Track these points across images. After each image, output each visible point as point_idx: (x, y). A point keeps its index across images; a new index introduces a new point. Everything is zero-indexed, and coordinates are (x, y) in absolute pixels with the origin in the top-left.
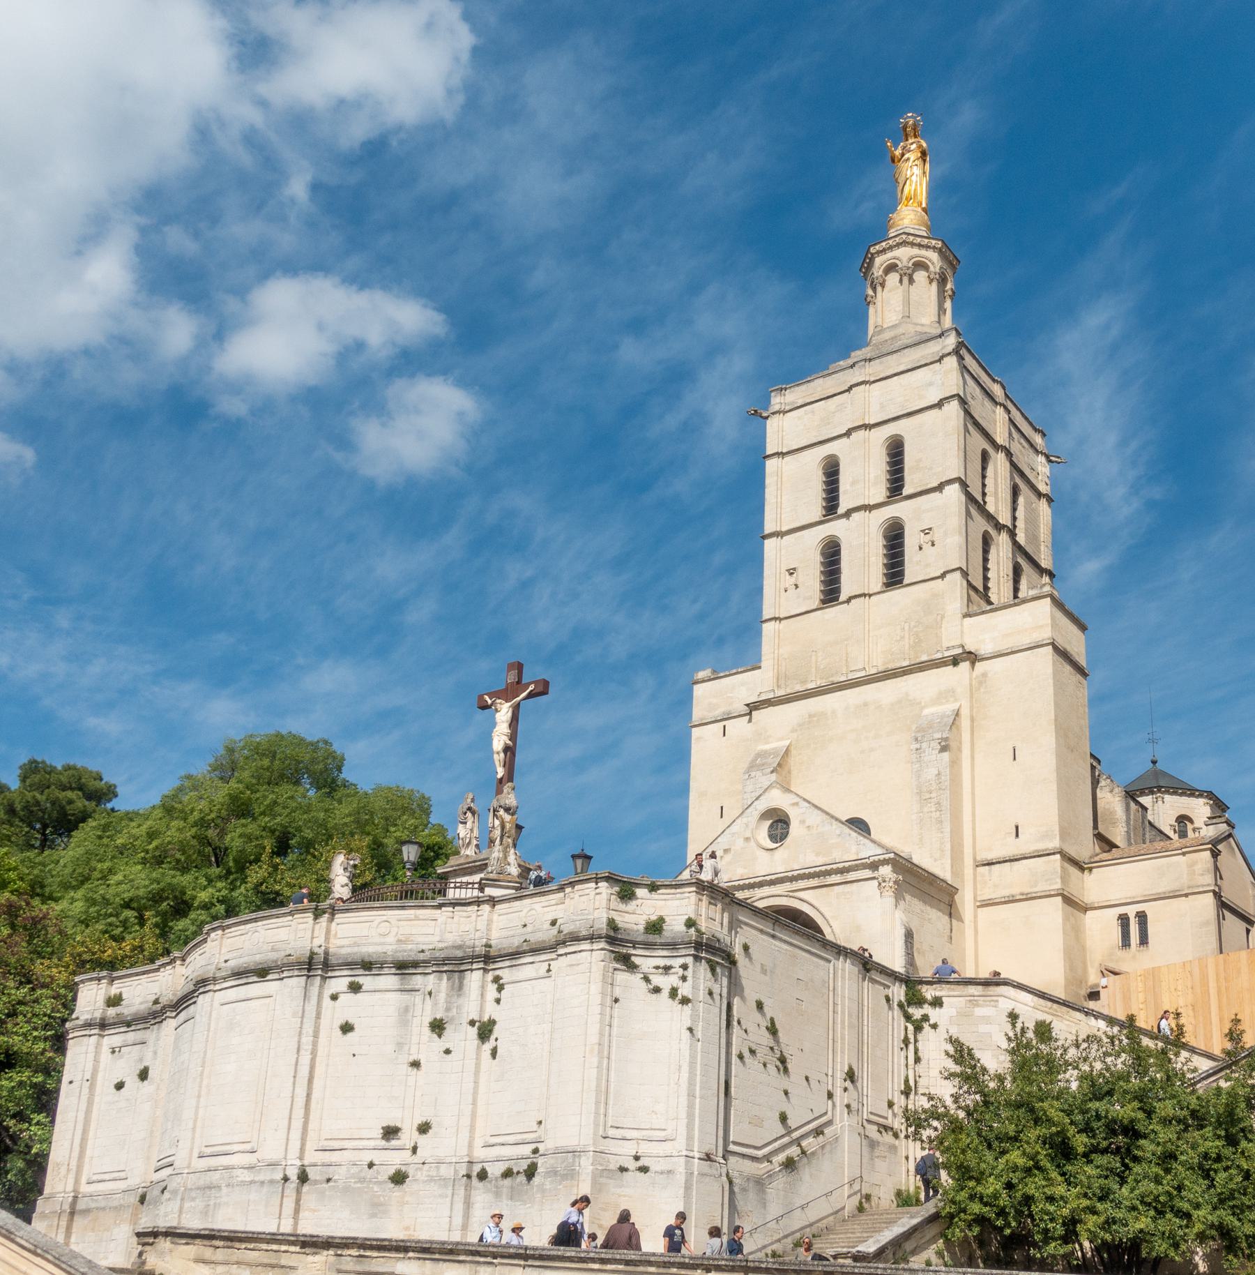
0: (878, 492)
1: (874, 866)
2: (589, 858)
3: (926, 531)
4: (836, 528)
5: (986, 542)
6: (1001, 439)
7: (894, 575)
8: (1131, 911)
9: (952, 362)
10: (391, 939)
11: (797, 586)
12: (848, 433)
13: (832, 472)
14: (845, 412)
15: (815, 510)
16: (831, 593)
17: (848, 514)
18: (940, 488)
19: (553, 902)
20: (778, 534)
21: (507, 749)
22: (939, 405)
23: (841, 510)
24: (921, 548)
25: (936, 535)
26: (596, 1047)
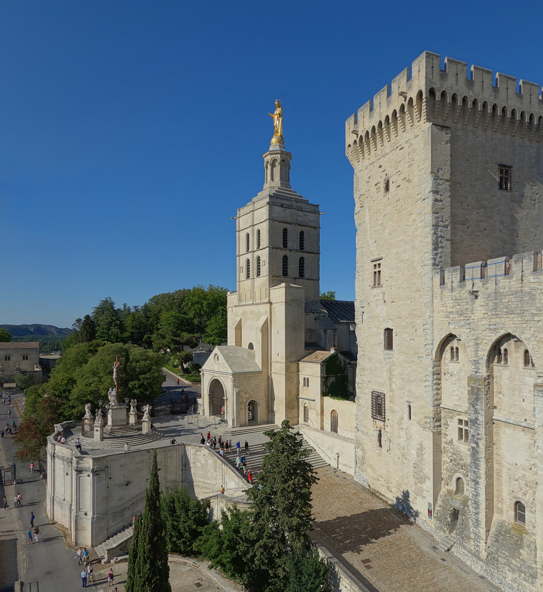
0: (256, 246)
5: (285, 259)
12: (250, 226)
18: (265, 248)
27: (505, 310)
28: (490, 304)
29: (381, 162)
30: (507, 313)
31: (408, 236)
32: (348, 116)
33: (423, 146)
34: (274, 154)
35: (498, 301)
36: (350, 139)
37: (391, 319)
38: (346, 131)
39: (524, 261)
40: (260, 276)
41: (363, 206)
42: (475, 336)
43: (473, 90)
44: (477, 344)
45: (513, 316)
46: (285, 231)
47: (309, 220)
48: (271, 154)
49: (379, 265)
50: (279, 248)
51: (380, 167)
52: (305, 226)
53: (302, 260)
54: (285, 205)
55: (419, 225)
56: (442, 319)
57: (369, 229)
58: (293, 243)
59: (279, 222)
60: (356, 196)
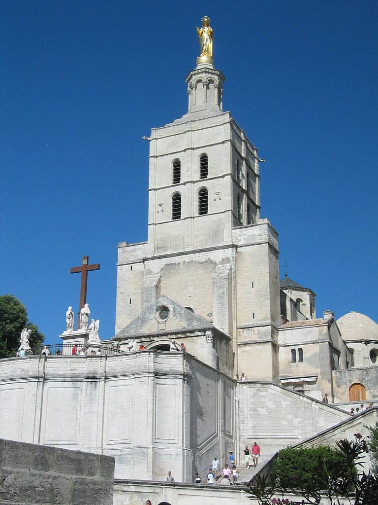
0: (197, 176)
1: (204, 330)
4: (178, 189)
6: (243, 155)
8: (297, 348)
9: (229, 125)
11: (163, 211)
12: (185, 151)
13: (177, 165)
14: (185, 142)
15: (170, 181)
16: (177, 214)
17: (184, 184)
18: (223, 177)
19: (131, 358)
20: (156, 190)
22: (223, 143)
23: (181, 182)
24: (215, 200)
25: (222, 195)
26: (152, 411)
34: (211, 73)
48: (206, 72)
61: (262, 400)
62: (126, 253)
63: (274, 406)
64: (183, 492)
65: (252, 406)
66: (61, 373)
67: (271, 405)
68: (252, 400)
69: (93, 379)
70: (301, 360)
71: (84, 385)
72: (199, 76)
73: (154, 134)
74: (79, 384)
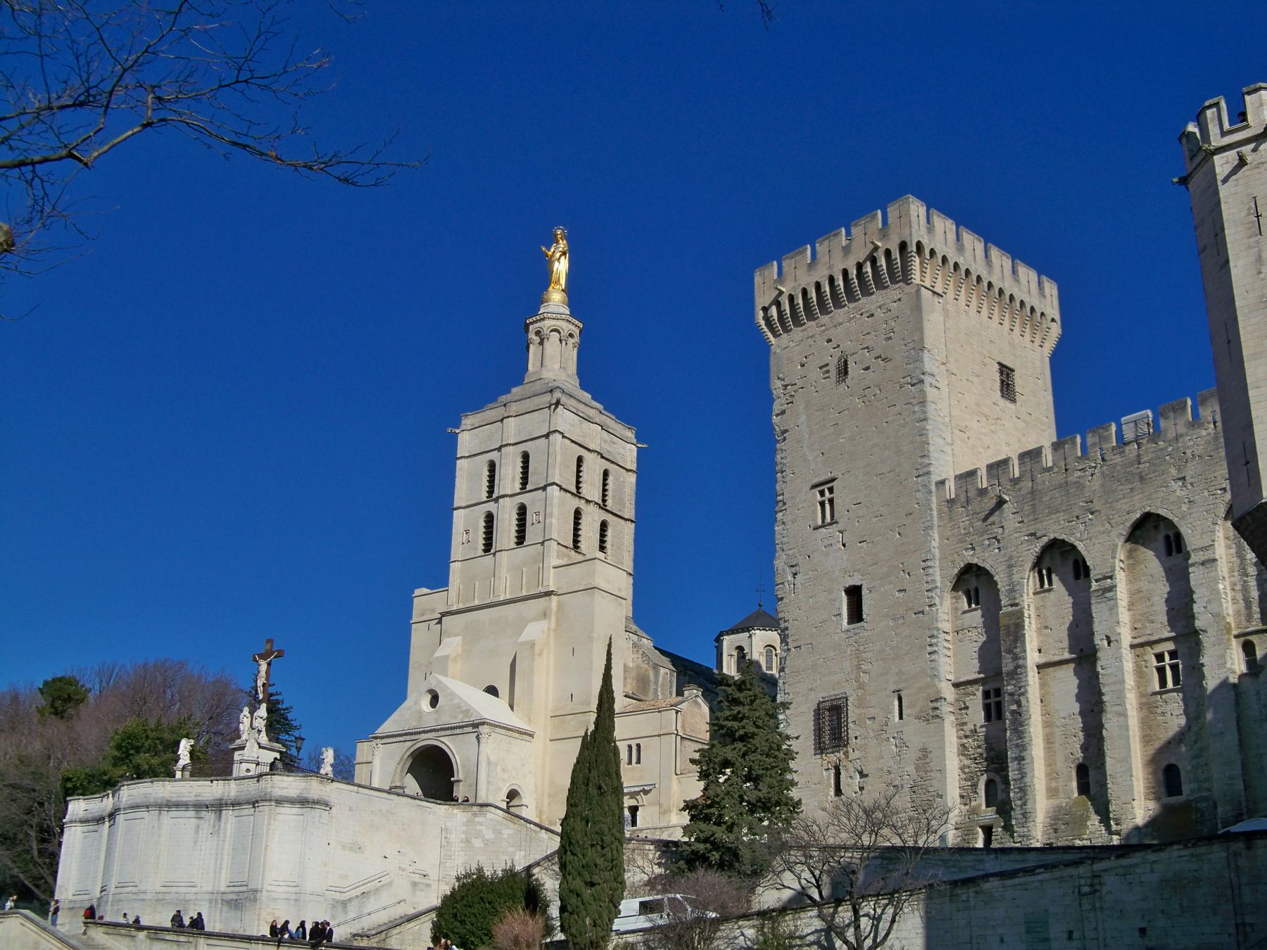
2: (304, 739)
3: (537, 514)
5: (578, 514)
7: (521, 538)
10: (193, 794)
12: (499, 449)
16: (488, 547)
21: (264, 685)
27: (1046, 511)
28: (1027, 508)
29: (832, 333)
30: (1050, 513)
31: (888, 438)
32: (763, 262)
33: (909, 313)
35: (1036, 501)
36: (763, 298)
37: (859, 570)
38: (756, 287)
39: (1066, 446)
40: (525, 544)
41: (792, 402)
42: (1008, 556)
43: (964, 257)
44: (1010, 566)
45: (1057, 515)
46: (580, 460)
47: (619, 453)
49: (831, 490)
50: (570, 492)
51: (829, 341)
52: (613, 462)
53: (604, 526)
54: (583, 413)
55: (907, 419)
56: (953, 547)
57: (807, 436)
58: (591, 490)
59: (573, 441)
60: (776, 385)
61: (478, 828)
62: (425, 602)
63: (493, 836)
64: (210, 942)
65: (463, 836)
66: (184, 799)
67: (489, 835)
68: (465, 828)
69: (219, 806)
70: (638, 762)
71: (209, 816)
72: (538, 325)
73: (468, 422)
74: (203, 814)
